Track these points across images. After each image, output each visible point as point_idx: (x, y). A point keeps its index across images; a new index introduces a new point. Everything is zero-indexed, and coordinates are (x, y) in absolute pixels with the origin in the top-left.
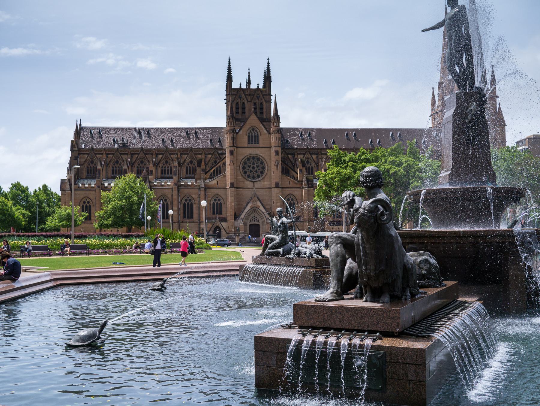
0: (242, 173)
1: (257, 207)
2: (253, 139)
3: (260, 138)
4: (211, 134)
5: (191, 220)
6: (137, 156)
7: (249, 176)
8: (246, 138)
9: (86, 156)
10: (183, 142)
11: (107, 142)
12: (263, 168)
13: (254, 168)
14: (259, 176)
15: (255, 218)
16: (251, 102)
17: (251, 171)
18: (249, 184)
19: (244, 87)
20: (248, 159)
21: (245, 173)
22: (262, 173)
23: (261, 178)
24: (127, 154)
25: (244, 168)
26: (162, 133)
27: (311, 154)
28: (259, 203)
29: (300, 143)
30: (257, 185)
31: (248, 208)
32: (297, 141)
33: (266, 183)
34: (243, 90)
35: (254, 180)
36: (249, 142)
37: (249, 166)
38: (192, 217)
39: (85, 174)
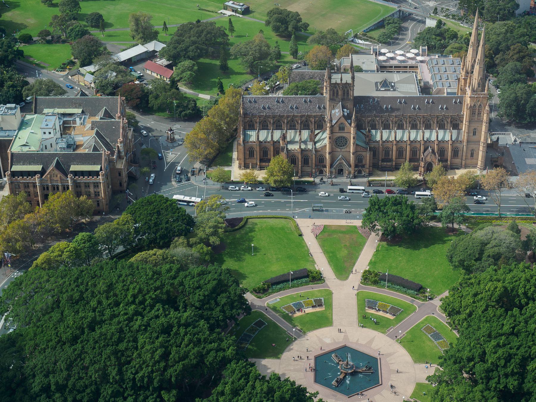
1: (342, 163)
8: (338, 128)
12: (347, 142)
14: (344, 146)
15: (341, 166)
18: (339, 150)
20: (339, 138)
21: (337, 144)
22: (346, 144)
25: (336, 142)
26: (289, 100)
30: (343, 150)
31: (338, 163)
34: (338, 84)
36: (339, 130)
38: (308, 164)
39: (248, 127)
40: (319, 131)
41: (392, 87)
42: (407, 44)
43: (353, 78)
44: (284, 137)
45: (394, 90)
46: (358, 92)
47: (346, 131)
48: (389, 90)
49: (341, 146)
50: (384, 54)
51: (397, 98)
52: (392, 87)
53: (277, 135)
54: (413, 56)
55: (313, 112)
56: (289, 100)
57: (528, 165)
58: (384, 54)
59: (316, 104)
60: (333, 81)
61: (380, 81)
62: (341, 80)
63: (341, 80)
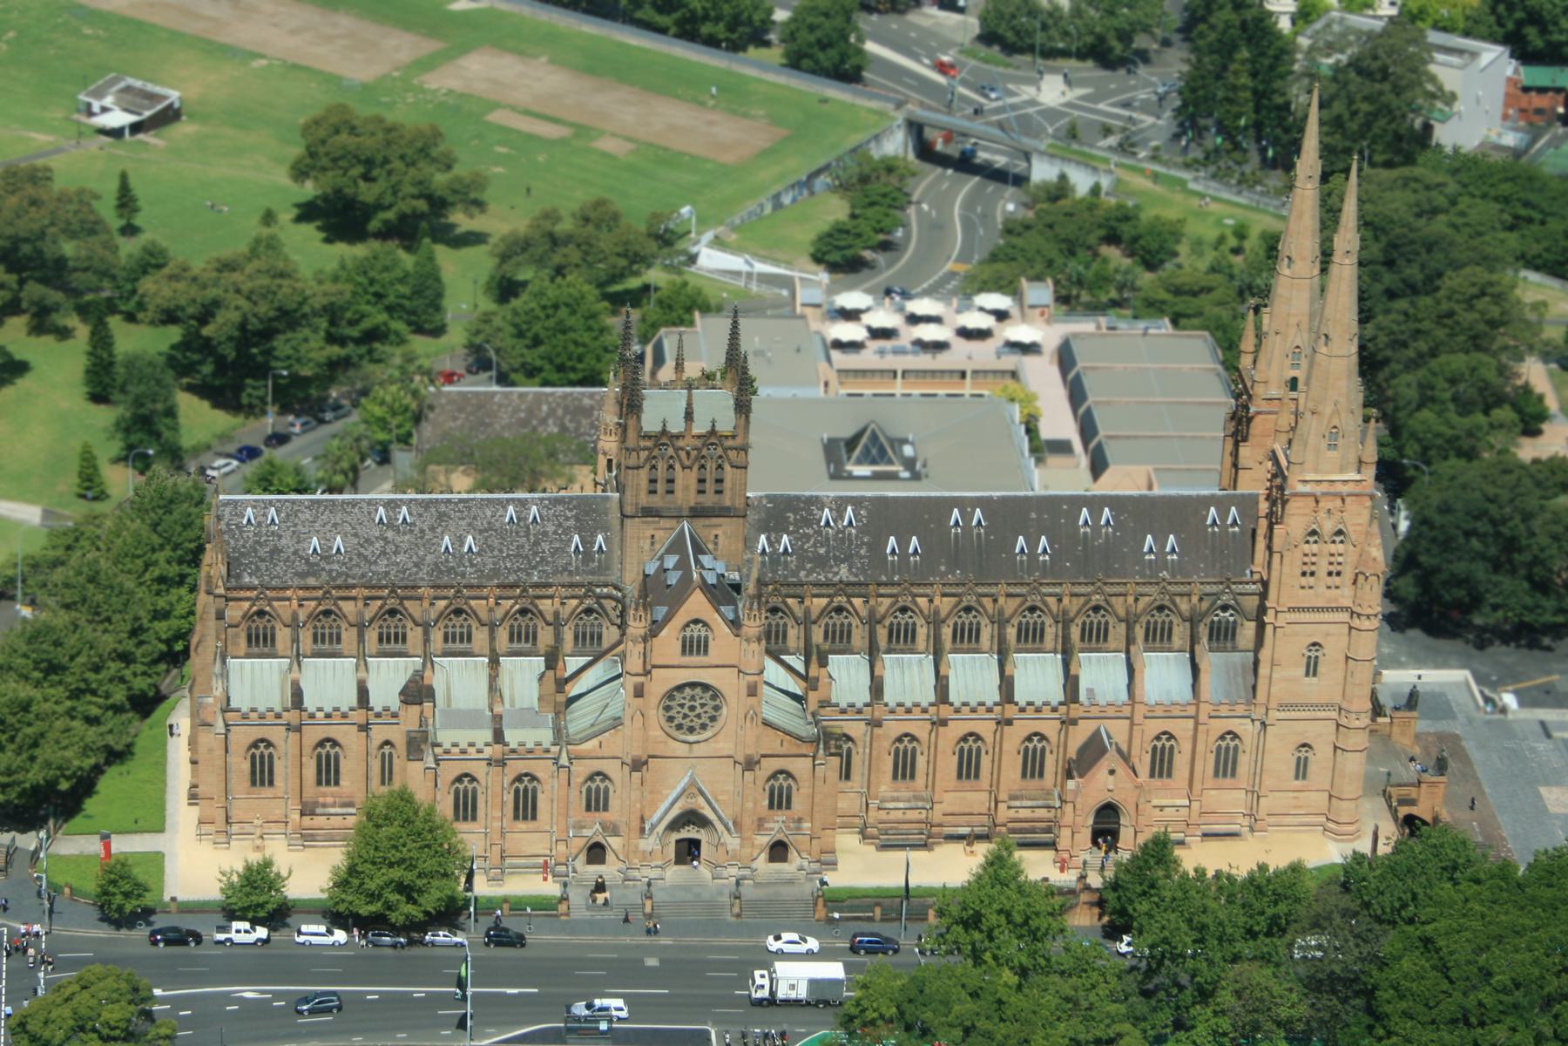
0: (663, 721)
2: (694, 646)
3: (711, 643)
4: (577, 519)
5: (531, 825)
6: (379, 603)
7: (679, 727)
9: (247, 605)
10: (501, 551)
11: (295, 553)
13: (692, 708)
14: (704, 727)
16: (690, 468)
17: (685, 716)
18: (681, 749)
19: (676, 426)
22: (713, 719)
23: (708, 733)
24: (354, 599)
26: (442, 516)
27: (849, 596)
28: (701, 800)
29: (822, 551)
30: (699, 750)
32: (814, 545)
33: (721, 745)
35: (691, 738)
36: (684, 652)
37: (682, 706)
40: (583, 660)
41: (909, 463)
42: (953, 274)
43: (743, 407)
44: (417, 693)
45: (916, 476)
46: (761, 482)
47: (714, 655)
48: (893, 477)
49: (691, 730)
50: (851, 315)
51: (948, 504)
52: (909, 463)
53: (388, 678)
54: (985, 322)
55: (555, 573)
56: (442, 516)
57: (1557, 817)
58: (851, 315)
59: (567, 531)
60: (650, 421)
61: (848, 433)
62: (689, 416)
63: (689, 416)
